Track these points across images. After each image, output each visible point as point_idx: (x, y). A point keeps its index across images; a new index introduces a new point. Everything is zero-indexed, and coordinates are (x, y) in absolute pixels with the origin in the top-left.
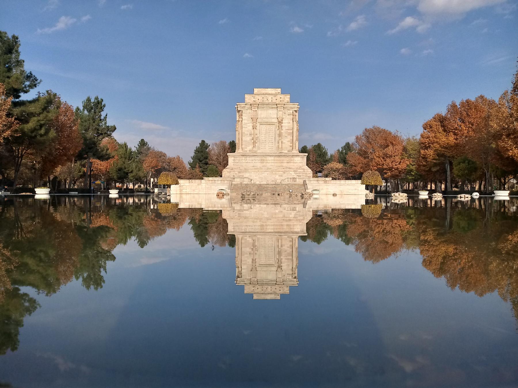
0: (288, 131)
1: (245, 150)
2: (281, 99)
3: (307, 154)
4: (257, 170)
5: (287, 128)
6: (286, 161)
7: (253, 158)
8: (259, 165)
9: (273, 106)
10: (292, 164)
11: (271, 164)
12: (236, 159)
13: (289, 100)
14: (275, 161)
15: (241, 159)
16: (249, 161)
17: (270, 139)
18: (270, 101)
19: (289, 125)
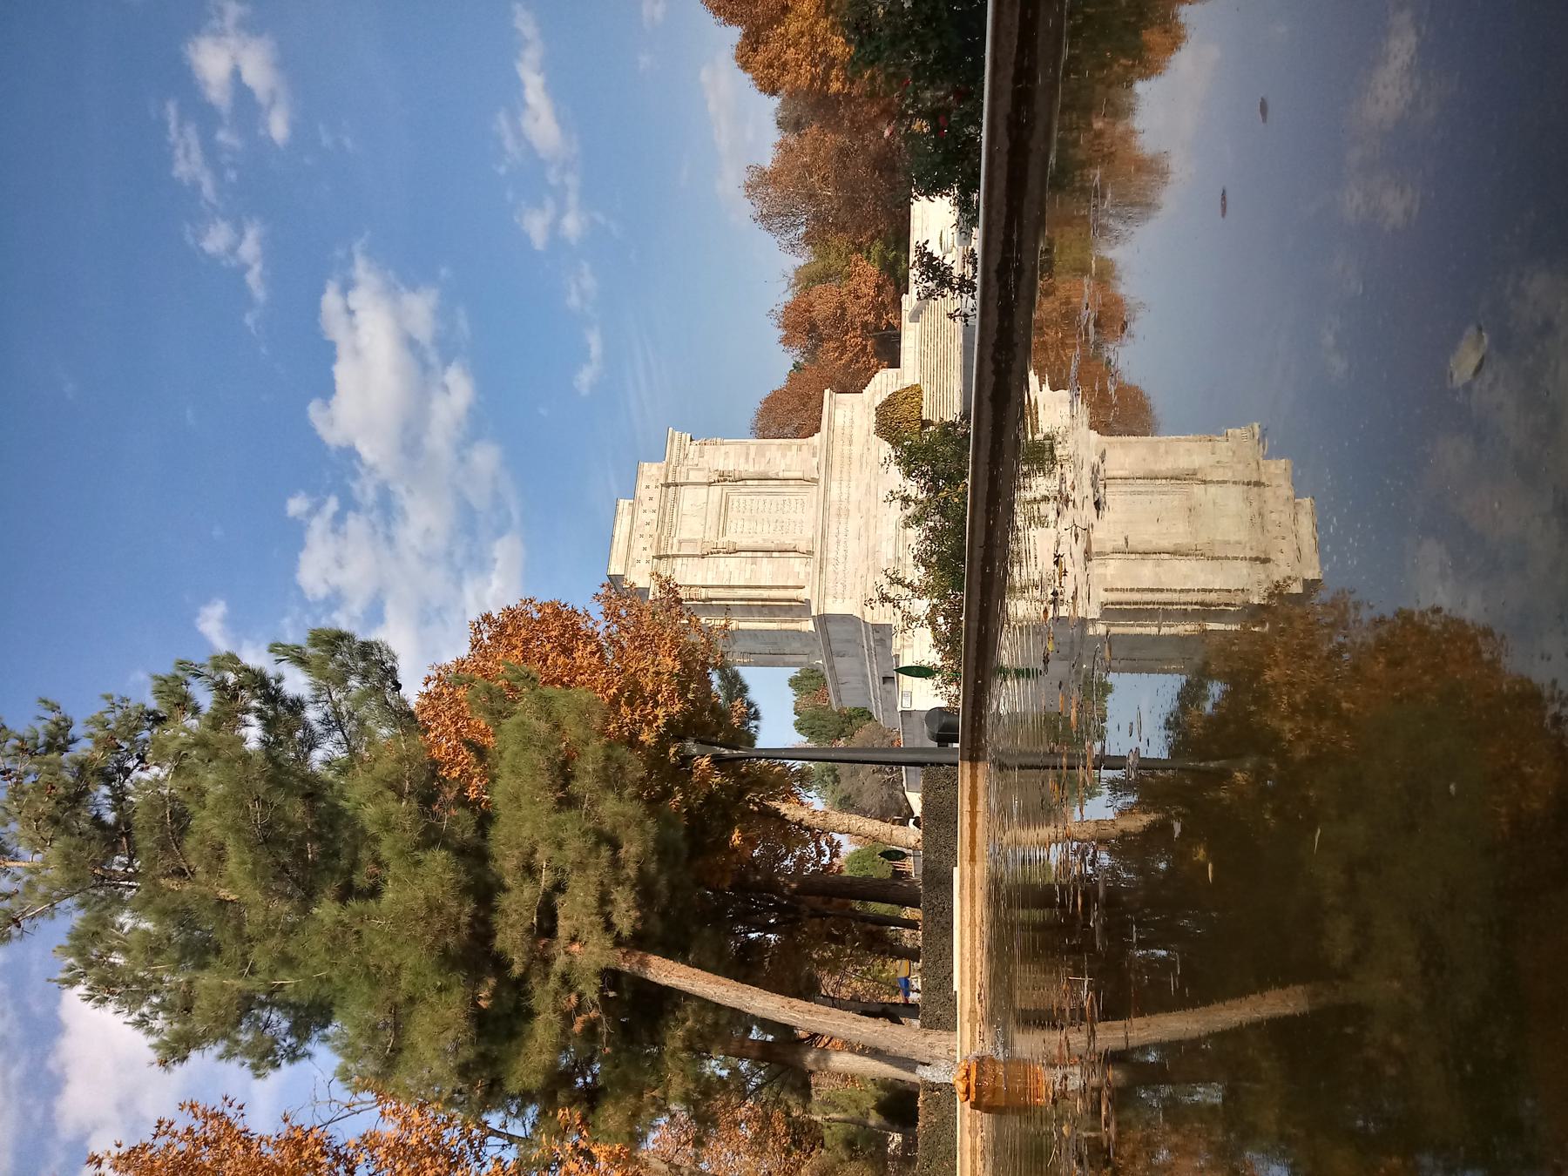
0: (752, 455)
1: (802, 576)
2: (652, 485)
3: (827, 392)
4: (872, 522)
5: (742, 460)
6: (846, 448)
7: (832, 541)
8: (854, 523)
9: (671, 496)
10: (855, 432)
11: (853, 490)
12: (831, 591)
13: (655, 466)
14: (845, 477)
15: (831, 576)
16: (841, 552)
17: (774, 508)
18: (654, 516)
19: (732, 454)
